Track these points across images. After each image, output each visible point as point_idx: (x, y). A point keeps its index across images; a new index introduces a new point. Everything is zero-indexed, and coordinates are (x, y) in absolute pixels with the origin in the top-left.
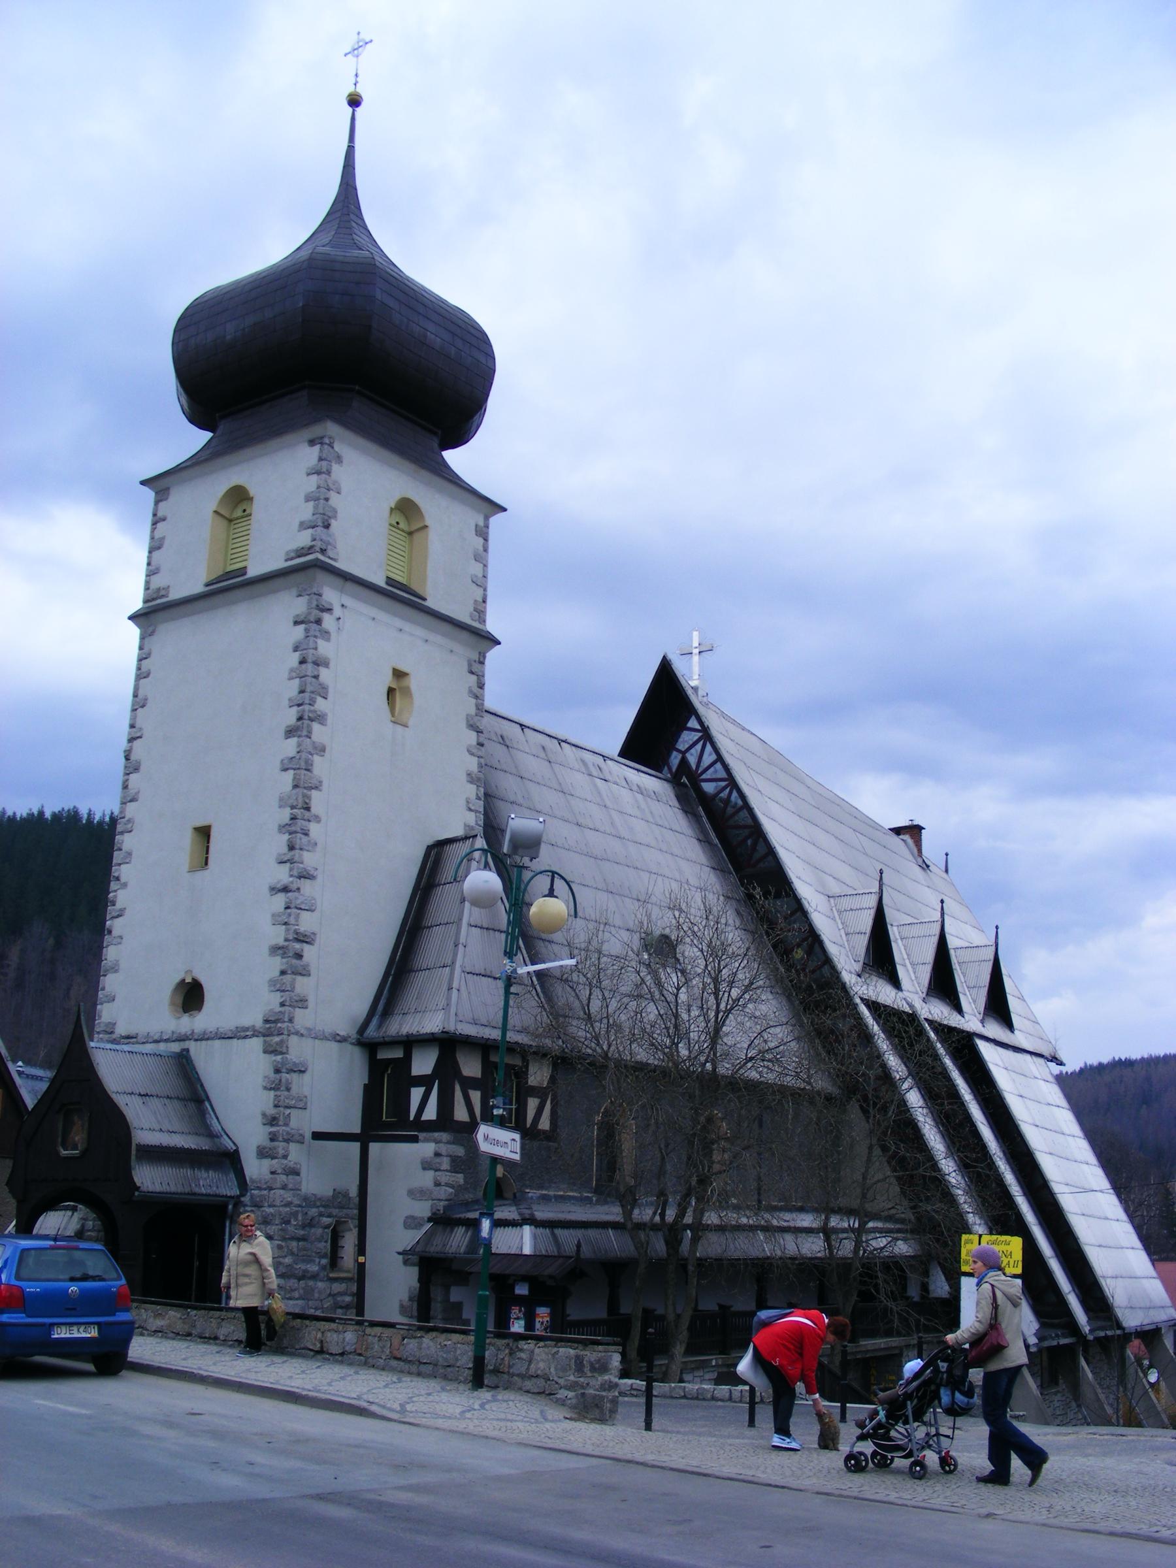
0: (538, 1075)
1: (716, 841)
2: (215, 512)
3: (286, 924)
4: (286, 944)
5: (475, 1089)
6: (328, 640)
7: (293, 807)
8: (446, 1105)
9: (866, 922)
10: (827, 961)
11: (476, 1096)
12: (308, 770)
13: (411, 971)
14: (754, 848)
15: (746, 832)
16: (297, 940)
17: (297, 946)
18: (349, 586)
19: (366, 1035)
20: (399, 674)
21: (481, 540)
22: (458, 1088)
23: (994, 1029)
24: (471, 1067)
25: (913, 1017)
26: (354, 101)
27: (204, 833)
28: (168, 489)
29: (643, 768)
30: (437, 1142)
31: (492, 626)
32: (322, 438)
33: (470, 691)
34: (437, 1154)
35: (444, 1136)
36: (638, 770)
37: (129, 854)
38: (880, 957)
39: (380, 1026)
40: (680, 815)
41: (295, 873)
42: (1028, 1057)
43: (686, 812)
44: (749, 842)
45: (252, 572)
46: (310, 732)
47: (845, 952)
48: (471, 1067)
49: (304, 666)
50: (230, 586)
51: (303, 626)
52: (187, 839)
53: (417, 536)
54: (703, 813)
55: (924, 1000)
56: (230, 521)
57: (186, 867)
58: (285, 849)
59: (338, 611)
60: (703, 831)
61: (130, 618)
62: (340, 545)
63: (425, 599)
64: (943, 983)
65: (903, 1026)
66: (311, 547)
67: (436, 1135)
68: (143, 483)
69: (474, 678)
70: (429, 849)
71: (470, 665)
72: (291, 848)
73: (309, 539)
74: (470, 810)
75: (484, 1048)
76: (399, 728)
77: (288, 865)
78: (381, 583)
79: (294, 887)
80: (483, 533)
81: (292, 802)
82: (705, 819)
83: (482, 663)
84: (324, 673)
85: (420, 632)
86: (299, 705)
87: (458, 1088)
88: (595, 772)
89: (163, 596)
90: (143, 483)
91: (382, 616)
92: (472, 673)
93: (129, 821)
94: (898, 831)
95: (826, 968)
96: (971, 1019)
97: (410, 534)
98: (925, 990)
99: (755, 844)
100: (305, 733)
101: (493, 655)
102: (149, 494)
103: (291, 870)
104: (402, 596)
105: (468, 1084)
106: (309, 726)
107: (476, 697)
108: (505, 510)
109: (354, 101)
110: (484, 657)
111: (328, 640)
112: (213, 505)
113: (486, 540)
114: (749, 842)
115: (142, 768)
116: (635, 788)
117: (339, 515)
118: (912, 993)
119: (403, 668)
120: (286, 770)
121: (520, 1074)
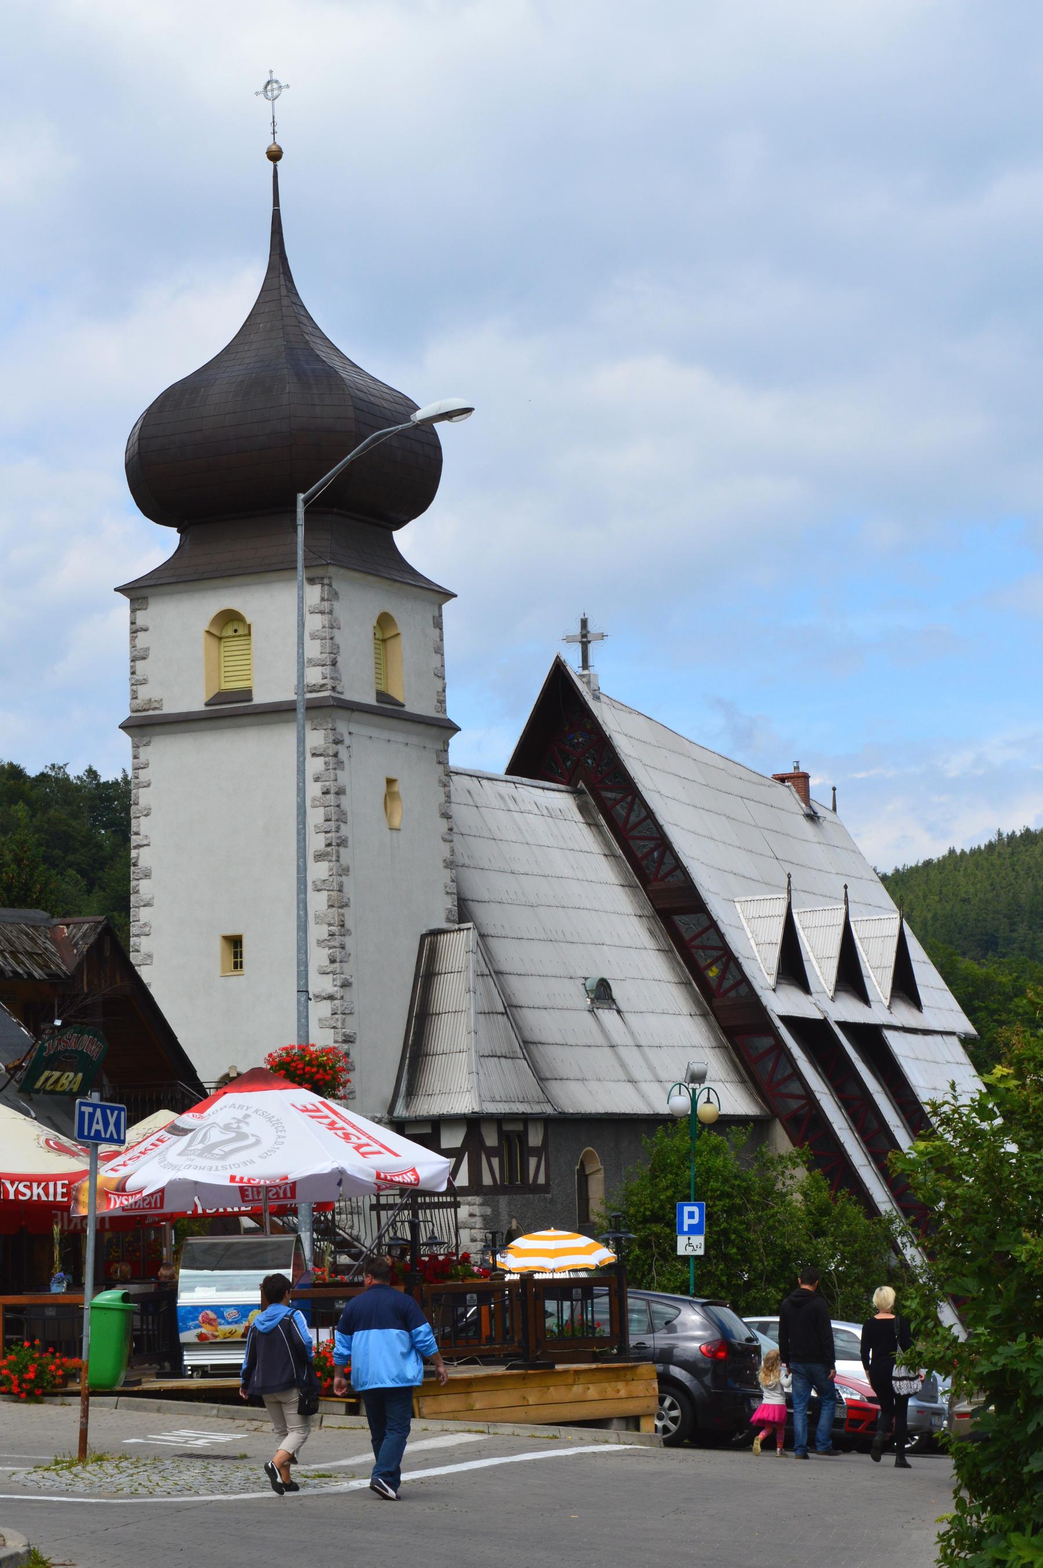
0: (535, 1138)
1: (620, 852)
2: (208, 632)
3: (334, 1027)
4: (336, 1045)
5: (495, 1156)
6: (343, 769)
7: (330, 925)
8: (475, 1173)
9: (777, 933)
10: (744, 980)
11: (495, 1162)
12: (340, 891)
13: (427, 1055)
14: (661, 862)
15: (651, 844)
16: (345, 1041)
17: (346, 1046)
18: (356, 715)
19: (395, 1115)
20: (390, 782)
21: (438, 630)
22: (484, 1157)
23: (904, 1015)
24: (491, 1140)
25: (822, 1025)
26: (275, 156)
27: (235, 943)
28: (145, 598)
29: (547, 784)
30: (469, 1204)
31: (452, 714)
32: (322, 578)
33: (440, 781)
34: (471, 1215)
35: (477, 1199)
36: (543, 788)
37: (150, 956)
38: (792, 968)
39: (407, 1106)
40: (584, 828)
41: (338, 983)
42: (938, 1038)
43: (589, 825)
44: (656, 854)
45: (260, 698)
46: (338, 857)
47: (760, 963)
48: (491, 1140)
49: (328, 796)
50: (231, 710)
51: (321, 760)
52: (217, 949)
53: (390, 643)
54: (603, 822)
55: (833, 999)
56: (220, 639)
57: (218, 971)
58: (327, 962)
59: (347, 742)
60: (607, 844)
61: (122, 727)
62: (343, 678)
63: (403, 706)
64: (850, 977)
65: (813, 1033)
66: (323, 686)
67: (470, 1198)
68: (116, 590)
69: (442, 766)
70: (423, 937)
71: (438, 756)
72: (333, 961)
73: (321, 676)
74: (448, 893)
75: (498, 1120)
76: (394, 833)
77: (331, 975)
78: (371, 700)
79: (338, 996)
80: (438, 624)
81: (327, 920)
82: (606, 828)
83: (446, 751)
84: (344, 801)
85: (401, 738)
86: (326, 832)
87: (484, 1157)
88: (512, 806)
89: (155, 709)
90: (116, 590)
91: (374, 732)
92: (440, 763)
93: (145, 925)
94: (782, 779)
95: (743, 990)
96: (878, 1009)
97: (384, 641)
98: (832, 988)
99: (662, 856)
100: (334, 858)
101: (455, 741)
102: (124, 602)
103: (334, 980)
104: (387, 710)
105: (491, 1152)
106: (338, 852)
107: (445, 786)
108: (456, 596)
109: (275, 156)
110: (448, 745)
111: (343, 769)
112: (206, 626)
113: (441, 629)
114: (656, 854)
115: (153, 875)
116: (545, 812)
117: (341, 650)
118: (824, 1002)
119: (393, 776)
120: (319, 890)
121: (523, 1137)
